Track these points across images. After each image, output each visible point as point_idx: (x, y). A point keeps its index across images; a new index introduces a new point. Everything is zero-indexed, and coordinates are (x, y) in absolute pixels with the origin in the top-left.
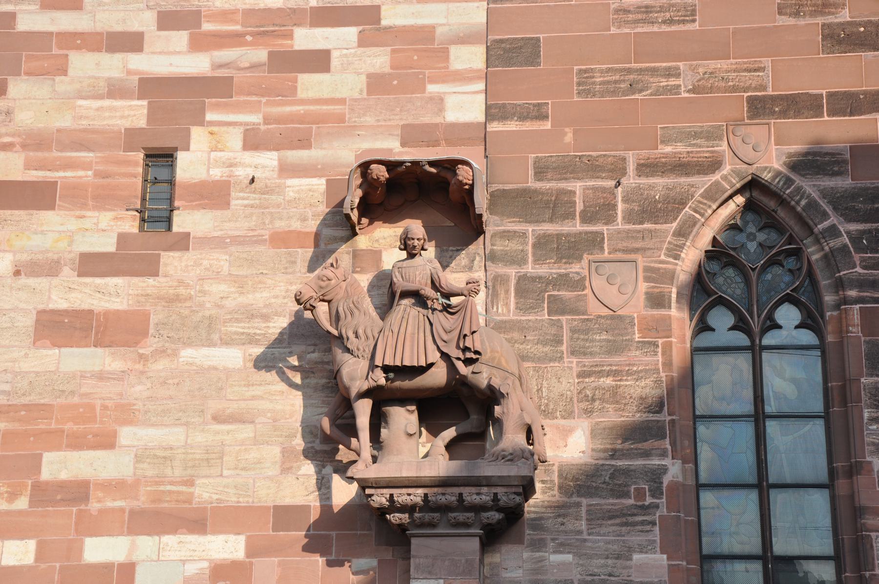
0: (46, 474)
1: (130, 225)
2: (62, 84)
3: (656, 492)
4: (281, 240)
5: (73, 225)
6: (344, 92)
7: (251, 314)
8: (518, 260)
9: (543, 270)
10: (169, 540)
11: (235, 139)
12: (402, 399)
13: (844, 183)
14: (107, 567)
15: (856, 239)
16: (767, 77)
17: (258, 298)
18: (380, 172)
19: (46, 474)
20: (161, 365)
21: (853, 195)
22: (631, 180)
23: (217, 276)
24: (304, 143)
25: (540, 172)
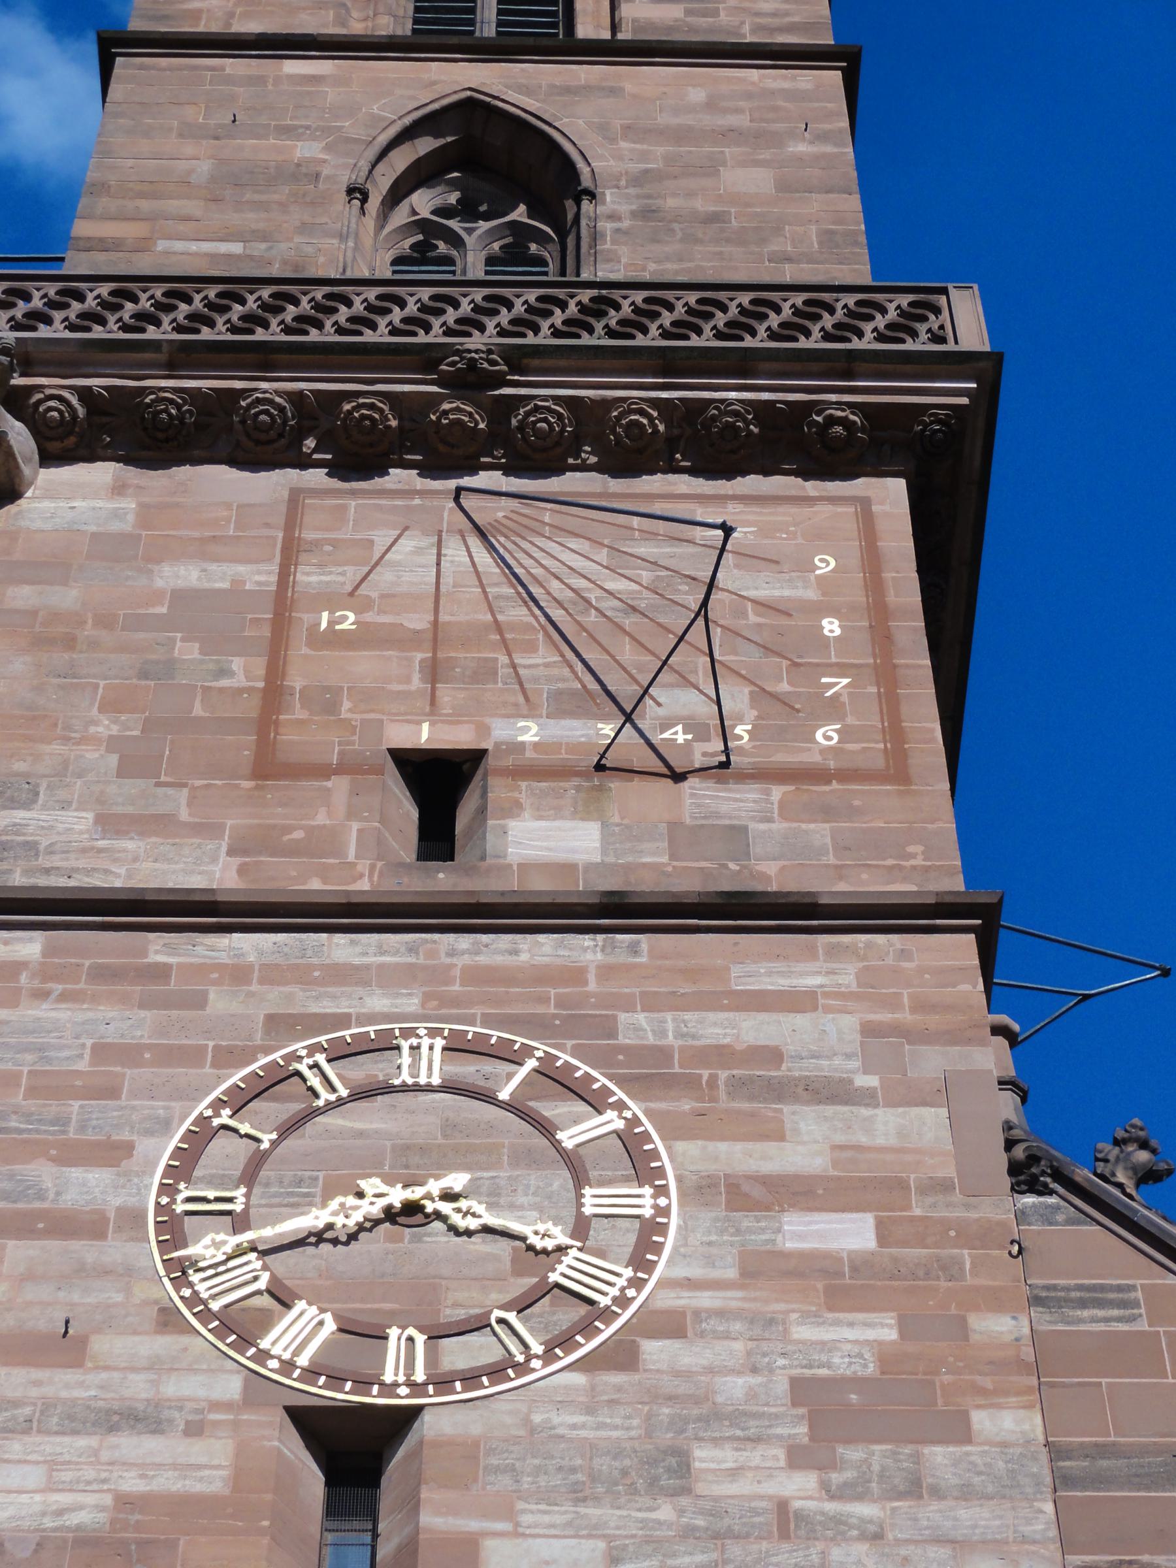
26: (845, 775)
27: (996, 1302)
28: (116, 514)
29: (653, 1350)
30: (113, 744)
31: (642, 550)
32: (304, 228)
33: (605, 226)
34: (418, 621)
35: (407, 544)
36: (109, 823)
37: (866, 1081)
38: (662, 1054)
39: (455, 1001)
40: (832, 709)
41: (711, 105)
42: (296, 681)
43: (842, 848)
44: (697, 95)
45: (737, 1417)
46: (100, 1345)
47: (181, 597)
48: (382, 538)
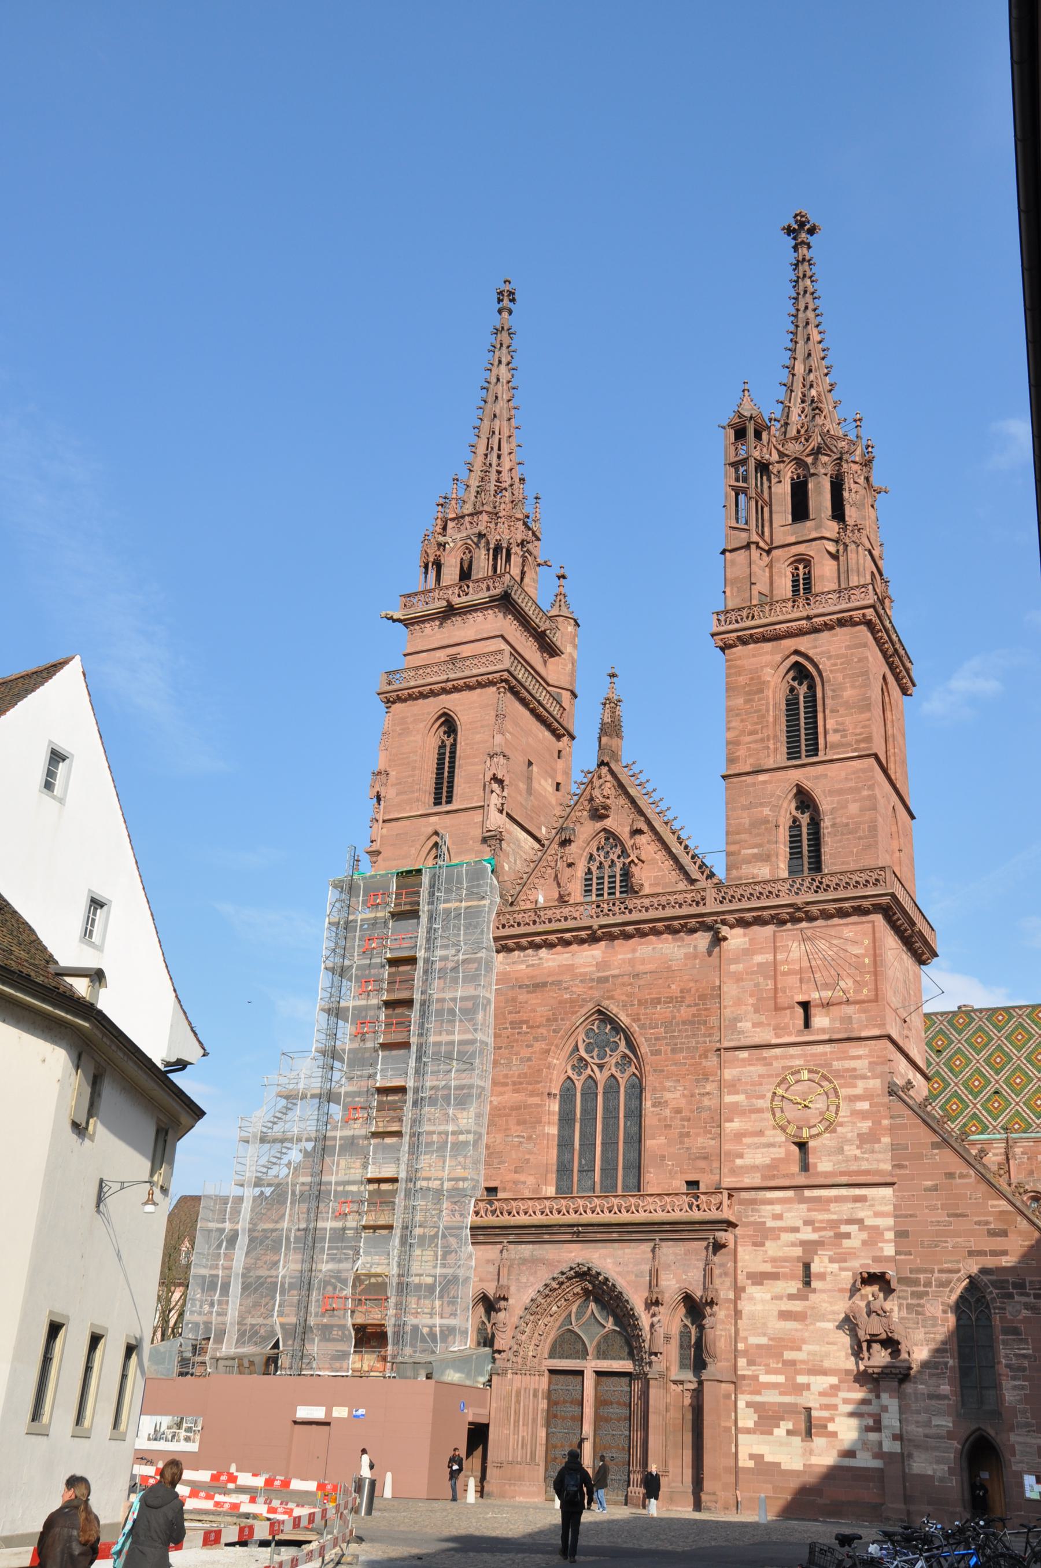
0: (785, 1357)
1: (800, 1286)
2: (779, 1242)
3: (946, 1368)
4: (841, 1290)
5: (785, 1285)
6: (855, 1245)
7: (834, 1313)
8: (906, 1298)
9: (914, 1302)
10: (818, 1377)
11: (826, 1260)
12: (876, 1341)
13: (994, 1278)
14: (803, 1384)
15: (997, 1294)
16: (972, 1244)
17: (836, 1308)
18: (865, 1275)
19: (785, 1357)
20: (811, 1327)
21: (996, 1281)
22: (936, 1275)
23: (824, 1301)
24: (845, 1261)
25: (911, 1272)
26: (869, 1001)
27: (885, 1118)
28: (745, 943)
29: (839, 1129)
30: (753, 1005)
31: (835, 942)
32: (769, 842)
33: (826, 831)
34: (797, 968)
35: (795, 945)
36: (754, 1025)
37: (869, 1074)
38: (839, 1070)
39: (808, 1061)
40: (866, 984)
41: (846, 779)
42: (779, 986)
43: (867, 1020)
44: (843, 774)
45: (850, 1141)
46: (767, 1133)
47: (759, 965)
48: (790, 943)
